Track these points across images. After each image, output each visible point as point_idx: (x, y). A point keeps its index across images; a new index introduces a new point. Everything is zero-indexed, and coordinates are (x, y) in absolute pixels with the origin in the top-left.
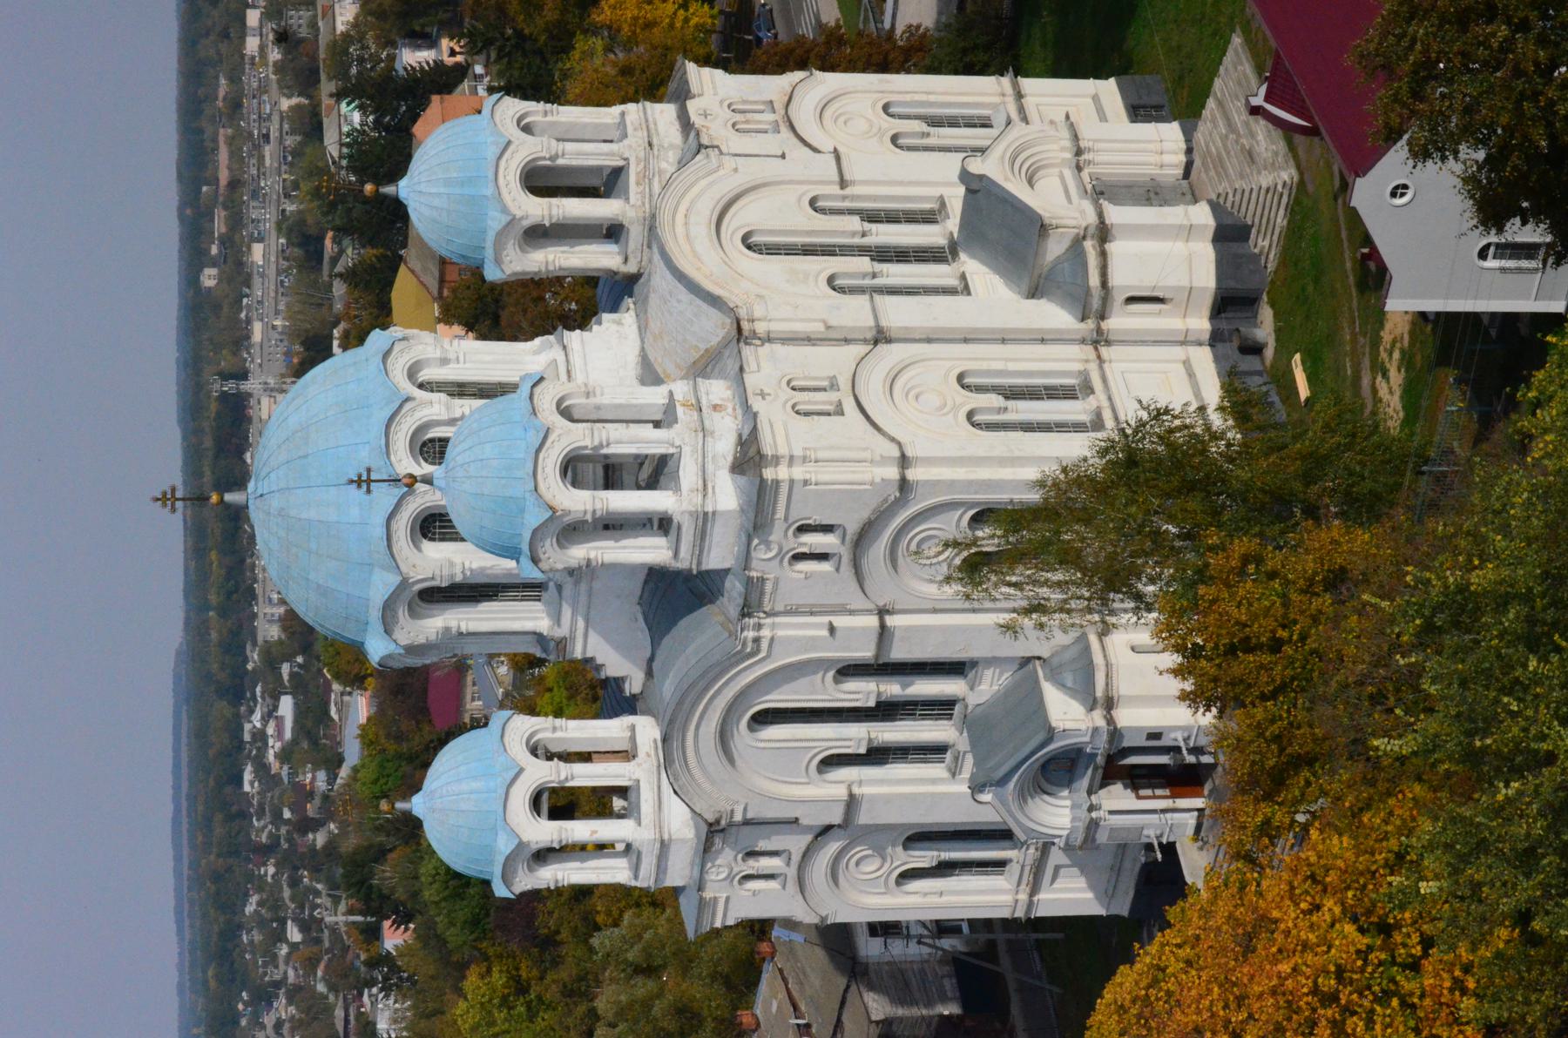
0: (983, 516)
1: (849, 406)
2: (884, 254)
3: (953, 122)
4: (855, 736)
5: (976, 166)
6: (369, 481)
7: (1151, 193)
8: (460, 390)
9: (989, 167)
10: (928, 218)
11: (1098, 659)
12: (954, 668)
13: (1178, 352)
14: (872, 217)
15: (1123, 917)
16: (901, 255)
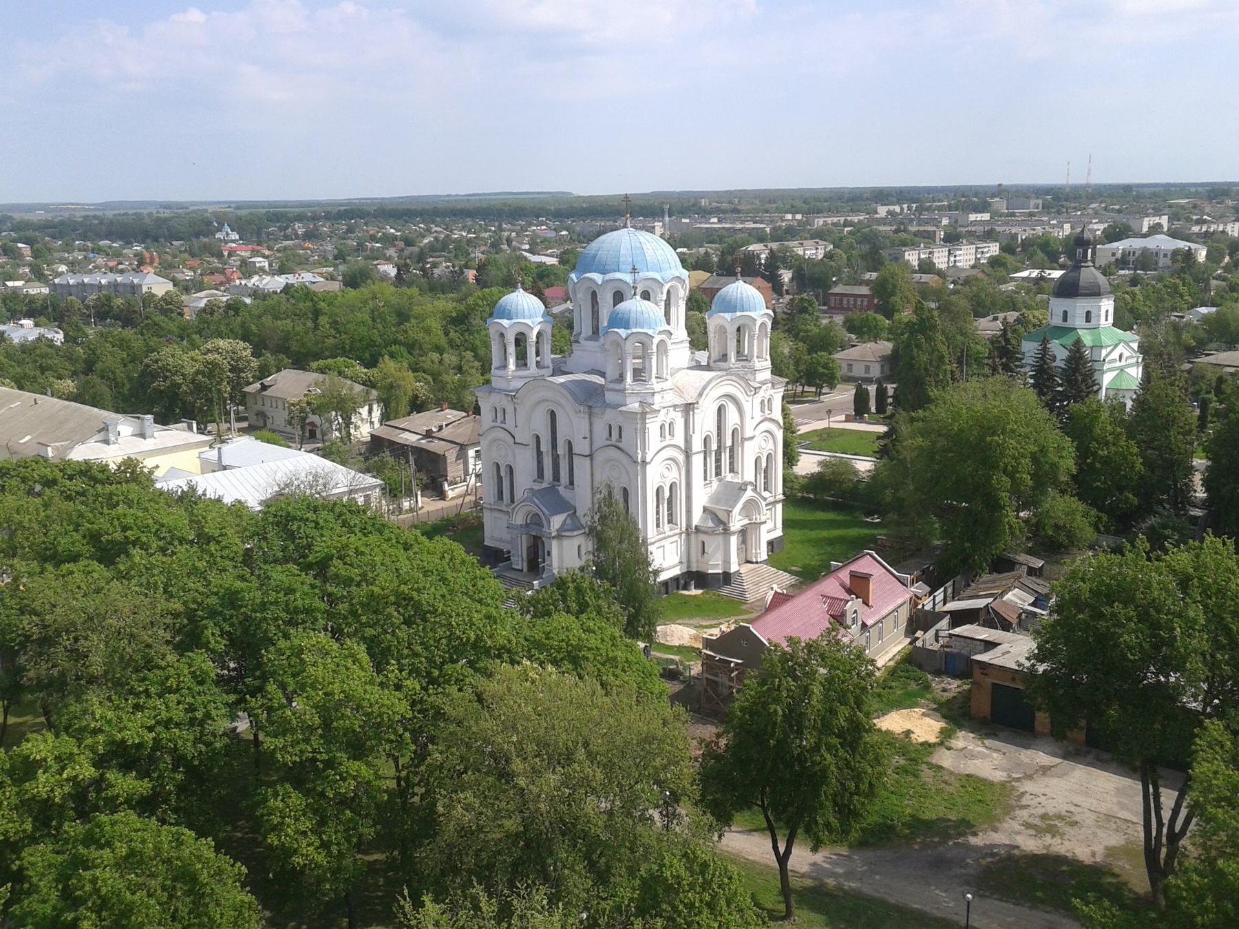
0: (625, 492)
3: (766, 477)
4: (545, 447)
5: (749, 488)
9: (749, 493)
10: (732, 470)
11: (575, 533)
12: (572, 483)
14: (732, 449)
16: (718, 460)
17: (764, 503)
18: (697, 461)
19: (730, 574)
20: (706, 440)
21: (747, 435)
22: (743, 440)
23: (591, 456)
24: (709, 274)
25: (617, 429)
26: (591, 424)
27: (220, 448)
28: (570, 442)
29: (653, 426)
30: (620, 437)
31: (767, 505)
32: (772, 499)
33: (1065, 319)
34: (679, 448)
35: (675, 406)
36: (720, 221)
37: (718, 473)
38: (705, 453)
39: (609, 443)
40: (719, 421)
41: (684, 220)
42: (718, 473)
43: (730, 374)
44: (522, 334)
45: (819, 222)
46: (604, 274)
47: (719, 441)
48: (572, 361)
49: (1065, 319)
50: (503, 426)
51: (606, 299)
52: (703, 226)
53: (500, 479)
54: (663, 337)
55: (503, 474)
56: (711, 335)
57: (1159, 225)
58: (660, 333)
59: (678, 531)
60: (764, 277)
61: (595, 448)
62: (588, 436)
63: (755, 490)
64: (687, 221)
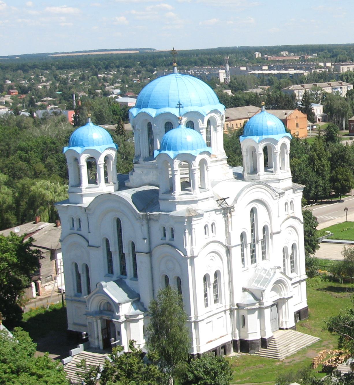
0: (179, 281)
3: (292, 262)
4: (114, 248)
6: (179, 107)
12: (136, 275)
15: (67, 327)
16: (253, 251)
17: (290, 282)
18: (236, 252)
19: (265, 339)
20: (243, 236)
21: (274, 231)
22: (273, 234)
23: (150, 253)
25: (170, 231)
26: (149, 228)
29: (198, 225)
30: (173, 236)
31: (293, 284)
32: (298, 279)
34: (221, 243)
35: (216, 210)
36: (270, 69)
38: (242, 245)
39: (164, 242)
40: (252, 220)
41: (242, 68)
43: (259, 184)
45: (344, 69)
46: (157, 109)
47: (253, 236)
48: (134, 178)
50: (79, 232)
51: (159, 127)
52: (257, 72)
53: (79, 276)
54: (205, 156)
55: (80, 272)
56: (244, 153)
58: (201, 153)
59: (224, 309)
60: (300, 109)
61: (153, 245)
62: (146, 236)
63: (284, 273)
64: (244, 68)
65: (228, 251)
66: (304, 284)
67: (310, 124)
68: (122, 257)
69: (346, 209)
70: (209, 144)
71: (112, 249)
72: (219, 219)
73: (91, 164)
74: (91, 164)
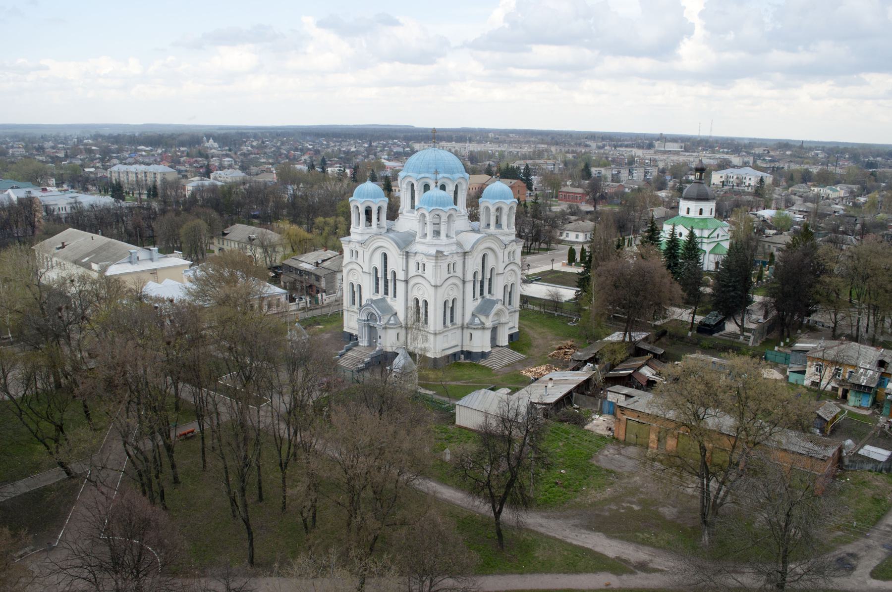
1: (450, 275)
2: (482, 283)
3: (510, 297)
7: (494, 339)
8: (456, 193)
9: (498, 306)
10: (490, 292)
12: (395, 296)
13: (460, 344)
14: (490, 280)
23: (406, 282)
24: (490, 177)
27: (370, 273)
28: (395, 273)
32: (513, 310)
33: (688, 213)
37: (482, 293)
42: (482, 293)
44: (369, 207)
49: (688, 213)
53: (354, 293)
55: (355, 289)
57: (748, 162)
65: (464, 282)
66: (517, 314)
67: (529, 192)
68: (386, 282)
69: (553, 260)
70: (455, 203)
71: (379, 275)
72: (459, 260)
73: (368, 212)
74: (368, 212)
